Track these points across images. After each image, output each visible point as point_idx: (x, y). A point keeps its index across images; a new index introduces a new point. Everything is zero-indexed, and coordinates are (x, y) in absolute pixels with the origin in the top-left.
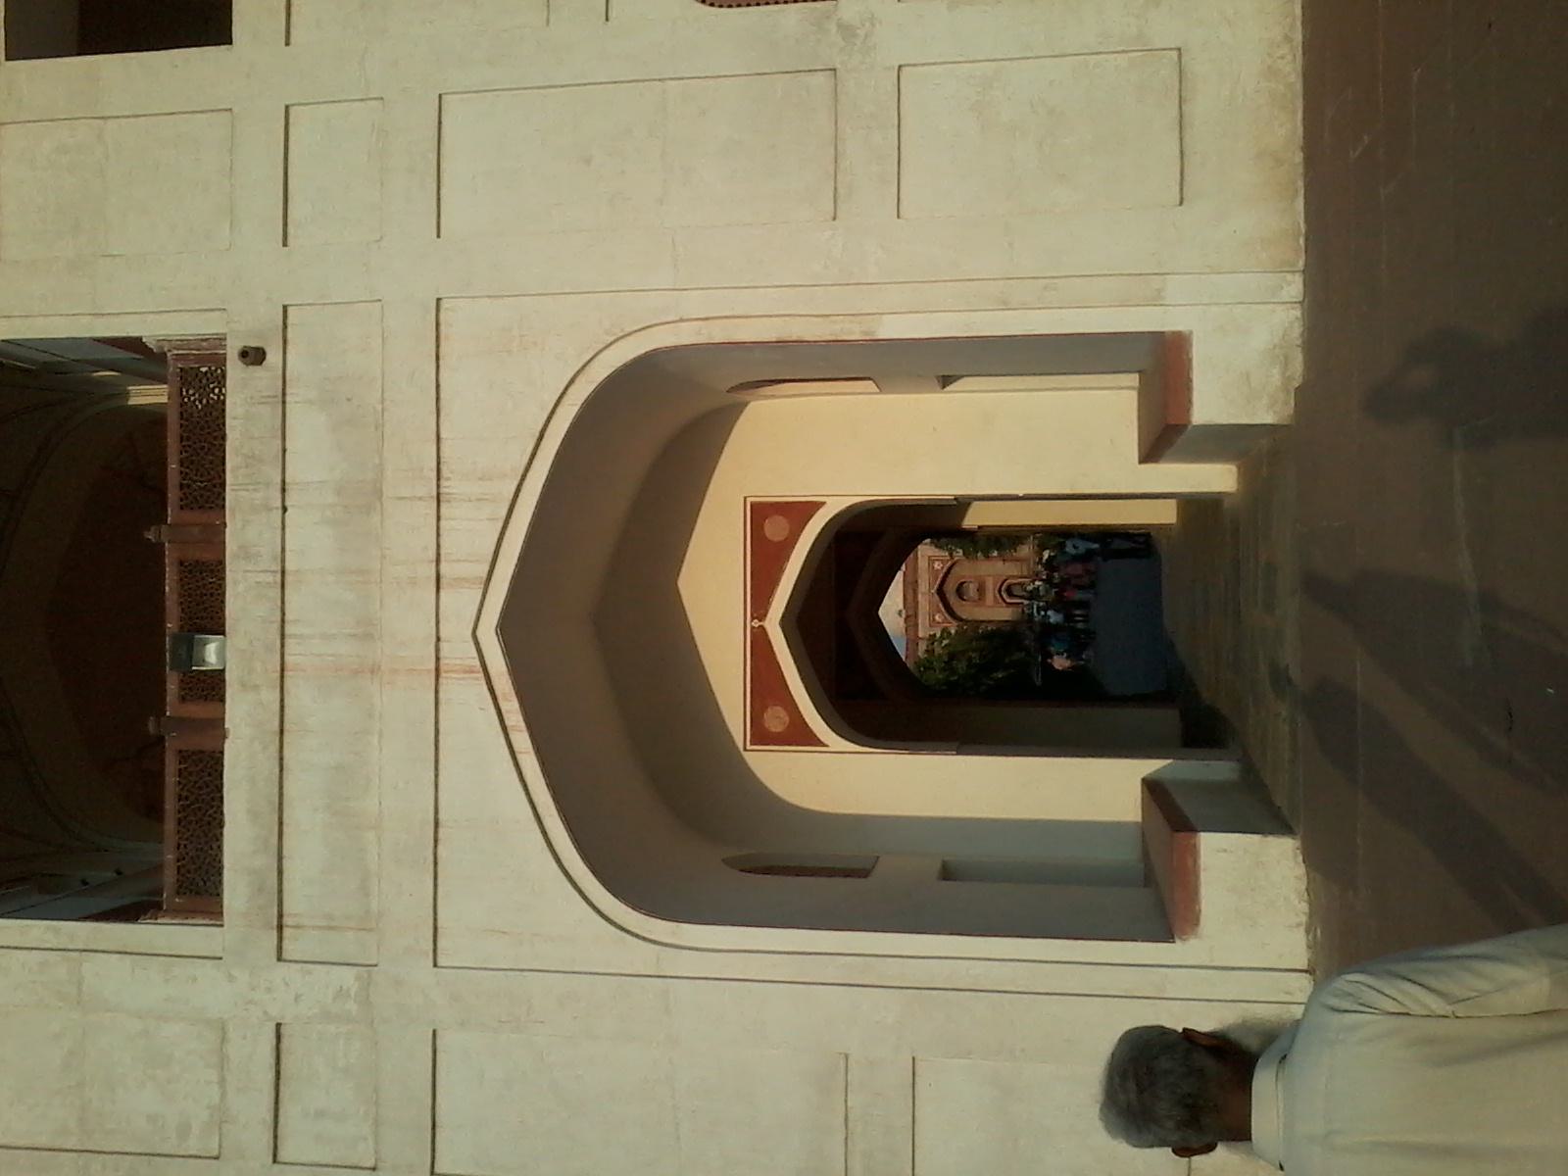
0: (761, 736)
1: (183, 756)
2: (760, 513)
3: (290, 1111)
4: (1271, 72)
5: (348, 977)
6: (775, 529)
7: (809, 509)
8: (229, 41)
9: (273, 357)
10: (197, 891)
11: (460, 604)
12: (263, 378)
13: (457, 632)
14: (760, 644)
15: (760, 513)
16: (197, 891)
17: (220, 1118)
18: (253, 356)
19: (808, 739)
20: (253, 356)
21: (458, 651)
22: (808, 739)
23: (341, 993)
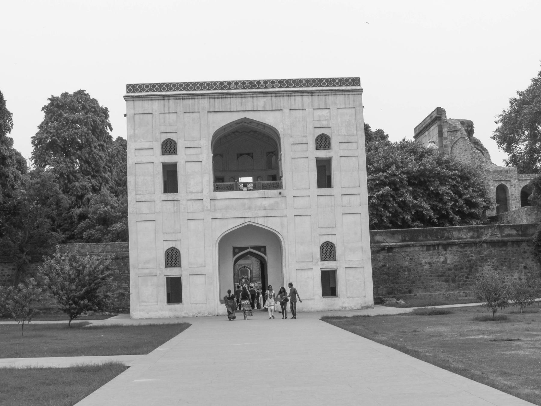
0: (234, 248)
1: (233, 184)
2: (265, 247)
3: (193, 201)
4: (312, 308)
5: (209, 208)
6: (263, 249)
7: (265, 254)
9: (280, 196)
10: (217, 189)
11: (252, 220)
12: (277, 194)
14: (247, 248)
15: (265, 247)
16: (217, 189)
17: (191, 193)
18: (280, 193)
20: (280, 193)
21: (247, 220)
23: (207, 207)
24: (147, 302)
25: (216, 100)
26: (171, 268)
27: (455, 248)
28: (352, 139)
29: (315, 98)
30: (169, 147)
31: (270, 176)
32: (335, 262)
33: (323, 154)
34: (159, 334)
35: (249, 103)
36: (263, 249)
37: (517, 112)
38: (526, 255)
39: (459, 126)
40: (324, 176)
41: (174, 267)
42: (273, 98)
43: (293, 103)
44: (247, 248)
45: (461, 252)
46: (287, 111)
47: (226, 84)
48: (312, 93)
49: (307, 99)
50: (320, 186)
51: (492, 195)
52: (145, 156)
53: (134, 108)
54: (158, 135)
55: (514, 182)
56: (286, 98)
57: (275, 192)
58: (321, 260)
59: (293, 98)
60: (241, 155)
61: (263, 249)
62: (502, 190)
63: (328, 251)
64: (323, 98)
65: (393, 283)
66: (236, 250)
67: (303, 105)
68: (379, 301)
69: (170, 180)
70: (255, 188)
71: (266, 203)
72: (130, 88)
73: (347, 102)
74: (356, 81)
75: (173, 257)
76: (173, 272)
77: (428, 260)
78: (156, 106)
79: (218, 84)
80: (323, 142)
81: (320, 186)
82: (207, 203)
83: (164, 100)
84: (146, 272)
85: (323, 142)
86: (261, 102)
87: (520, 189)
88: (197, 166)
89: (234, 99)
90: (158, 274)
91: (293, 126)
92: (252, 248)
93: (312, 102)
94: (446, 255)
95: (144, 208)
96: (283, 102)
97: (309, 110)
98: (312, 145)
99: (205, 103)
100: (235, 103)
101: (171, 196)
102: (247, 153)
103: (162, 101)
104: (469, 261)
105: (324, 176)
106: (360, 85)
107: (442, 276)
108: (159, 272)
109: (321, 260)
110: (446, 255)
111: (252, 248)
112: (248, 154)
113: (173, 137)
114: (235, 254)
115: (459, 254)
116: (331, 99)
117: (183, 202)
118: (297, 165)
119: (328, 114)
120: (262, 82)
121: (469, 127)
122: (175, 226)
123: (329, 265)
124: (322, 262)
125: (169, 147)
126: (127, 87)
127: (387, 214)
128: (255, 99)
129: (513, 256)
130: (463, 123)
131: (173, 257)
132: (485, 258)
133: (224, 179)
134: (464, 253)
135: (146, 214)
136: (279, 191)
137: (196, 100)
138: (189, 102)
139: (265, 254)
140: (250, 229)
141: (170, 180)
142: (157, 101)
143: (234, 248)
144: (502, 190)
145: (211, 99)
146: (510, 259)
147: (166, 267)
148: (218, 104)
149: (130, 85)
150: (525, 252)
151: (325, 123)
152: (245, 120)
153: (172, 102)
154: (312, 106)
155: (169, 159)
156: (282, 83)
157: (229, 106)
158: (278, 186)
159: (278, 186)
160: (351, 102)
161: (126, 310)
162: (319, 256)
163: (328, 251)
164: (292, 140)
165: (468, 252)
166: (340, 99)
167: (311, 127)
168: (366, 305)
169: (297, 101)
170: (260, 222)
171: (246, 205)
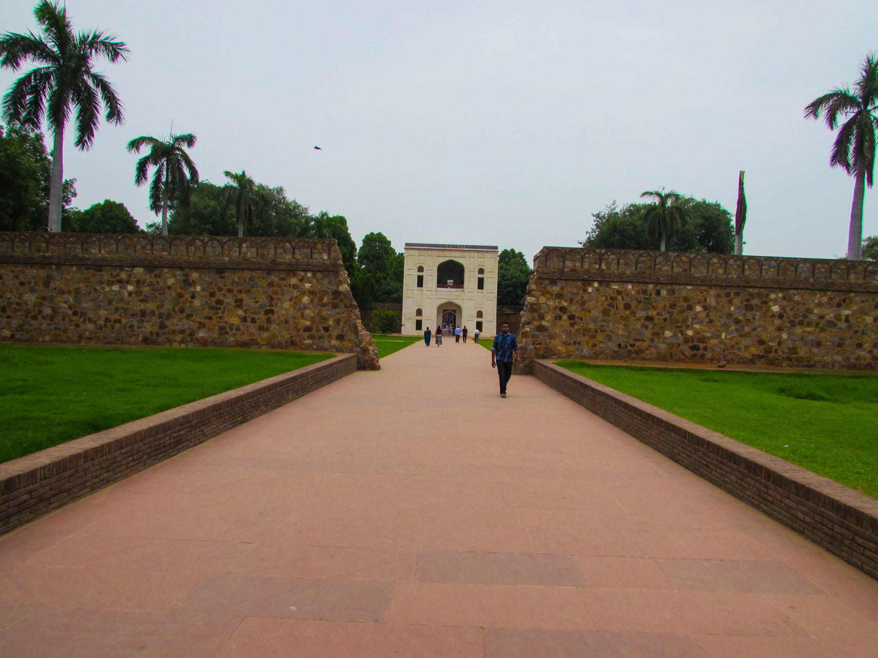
24: (408, 328)
30: (421, 269)
31: (459, 283)
33: (481, 276)
34: (412, 340)
35: (453, 254)
36: (455, 311)
40: (481, 284)
49: (476, 254)
61: (455, 311)
63: (480, 314)
69: (420, 282)
70: (453, 287)
71: (457, 293)
72: (407, 244)
75: (419, 312)
76: (419, 318)
78: (416, 252)
80: (481, 271)
82: (434, 292)
85: (481, 271)
86: (458, 254)
88: (431, 277)
91: (470, 264)
95: (409, 292)
96: (467, 254)
98: (477, 272)
99: (435, 253)
100: (447, 254)
102: (451, 274)
105: (481, 284)
116: (486, 254)
118: (470, 279)
122: (421, 300)
123: (480, 320)
125: (421, 269)
131: (419, 312)
133: (441, 283)
140: (450, 304)
141: (420, 282)
148: (441, 253)
155: (420, 274)
156: (467, 247)
158: (462, 287)
161: (400, 332)
163: (480, 314)
166: (489, 254)
169: (472, 254)
170: (454, 301)
171: (449, 294)
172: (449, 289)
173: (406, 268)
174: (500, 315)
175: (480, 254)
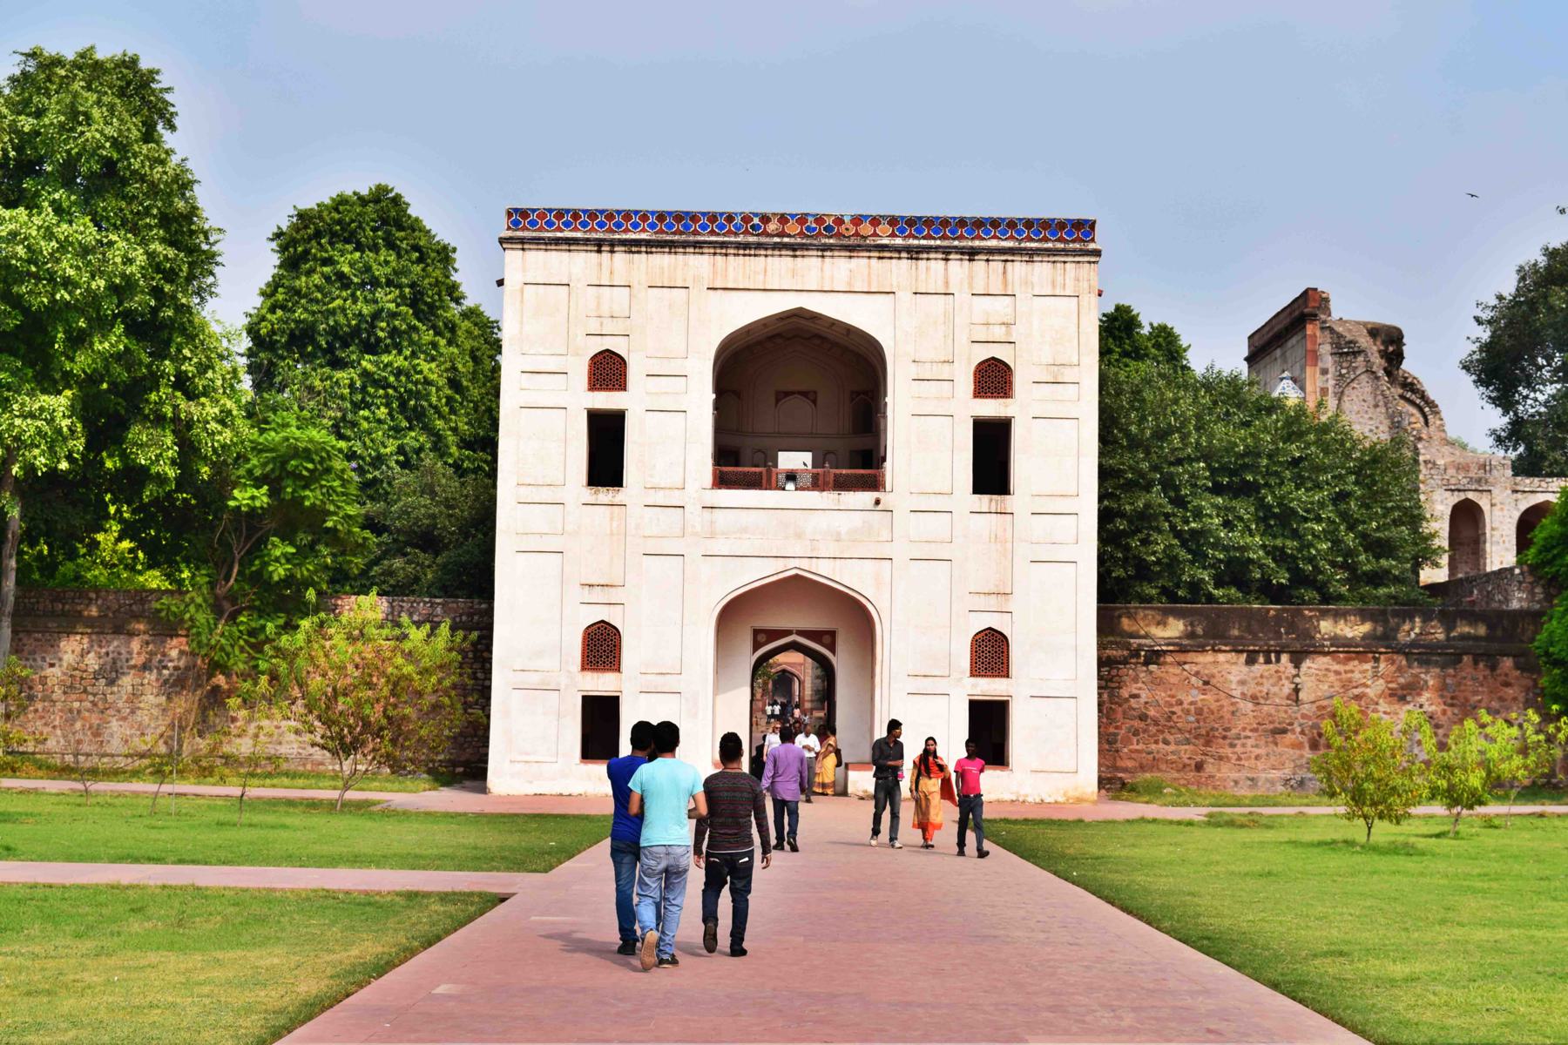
0: (756, 632)
2: (832, 634)
5: (698, 528)
6: (827, 639)
7: (833, 652)
8: (976, 491)
10: (721, 481)
11: (804, 564)
12: (870, 505)
13: (796, 562)
14: (788, 633)
15: (832, 634)
16: (721, 481)
18: (878, 502)
19: (755, 650)
20: (878, 502)
22: (755, 650)
25: (731, 258)
26: (595, 675)
27: (1323, 661)
28: (1068, 375)
29: (979, 265)
31: (857, 459)
32: (1004, 680)
33: (991, 408)
36: (828, 638)
37: (1532, 305)
38: (1510, 691)
39: (1364, 341)
41: (604, 670)
42: (874, 261)
43: (922, 276)
44: (788, 633)
45: (1337, 673)
46: (905, 296)
47: (756, 221)
48: (972, 254)
49: (958, 268)
50: (980, 487)
51: (1439, 526)
52: (547, 391)
53: (524, 270)
54: (580, 339)
55: (1501, 494)
56: (905, 264)
57: (866, 497)
58: (972, 675)
59: (922, 264)
60: (787, 394)
61: (828, 638)
62: (1467, 517)
63: (991, 652)
64: (996, 266)
65: (1156, 742)
66: (761, 636)
67: (947, 283)
68: (1112, 783)
70: (817, 484)
72: (518, 216)
73: (1059, 279)
74: (1084, 228)
75: (602, 646)
77: (1251, 689)
78: (579, 265)
79: (738, 220)
80: (993, 378)
81: (980, 487)
83: (599, 251)
84: (533, 679)
85: (993, 378)
86: (841, 269)
87: (1517, 515)
88: (674, 424)
89: (777, 259)
90: (562, 687)
92: (800, 633)
93: (971, 277)
94: (1297, 680)
97: (962, 296)
98: (966, 383)
99: (697, 266)
101: (605, 495)
103: (594, 255)
104: (1358, 698)
106: (1093, 240)
107: (1284, 731)
108: (563, 681)
109: (972, 675)
110: (1297, 680)
111: (800, 633)
112: (804, 394)
113: (618, 346)
114: (756, 647)
115: (1332, 677)
116: (1018, 268)
117: (635, 511)
118: (925, 430)
119: (1010, 310)
120: (847, 219)
121: (1391, 342)
123: (989, 688)
124: (974, 680)
125: (608, 370)
126: (509, 214)
127: (1128, 576)
128: (827, 260)
129: (1475, 693)
130: (1374, 332)
131: (602, 646)
132: (1400, 692)
133: (738, 460)
134: (1344, 676)
135: (541, 534)
136: (875, 495)
137: (680, 257)
138: (662, 262)
139: (833, 652)
140: (797, 588)
142: (583, 254)
143: (756, 632)
144: (1467, 517)
145: (718, 258)
146: (1467, 700)
147: (583, 669)
148: (737, 268)
149: (516, 210)
150: (1507, 684)
151: (998, 333)
152: (799, 314)
153: (620, 258)
154: (971, 286)
155: (606, 400)
157: (761, 277)
158: (874, 484)
159: (874, 484)
160: (1070, 283)
162: (965, 663)
163: (991, 652)
164: (914, 371)
165: (1357, 675)
166: (1041, 272)
167: (963, 339)
168: (1077, 794)
169: (933, 270)
172: (790, 496)
173: (510, 364)
174: (1117, 659)
175: (984, 272)
